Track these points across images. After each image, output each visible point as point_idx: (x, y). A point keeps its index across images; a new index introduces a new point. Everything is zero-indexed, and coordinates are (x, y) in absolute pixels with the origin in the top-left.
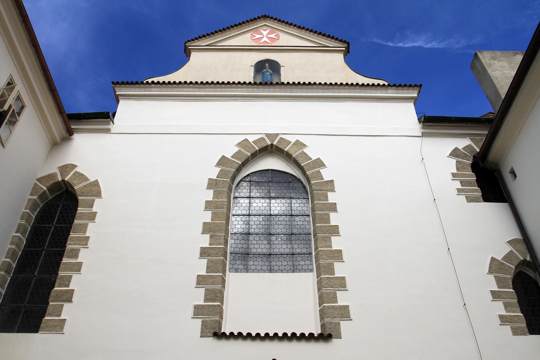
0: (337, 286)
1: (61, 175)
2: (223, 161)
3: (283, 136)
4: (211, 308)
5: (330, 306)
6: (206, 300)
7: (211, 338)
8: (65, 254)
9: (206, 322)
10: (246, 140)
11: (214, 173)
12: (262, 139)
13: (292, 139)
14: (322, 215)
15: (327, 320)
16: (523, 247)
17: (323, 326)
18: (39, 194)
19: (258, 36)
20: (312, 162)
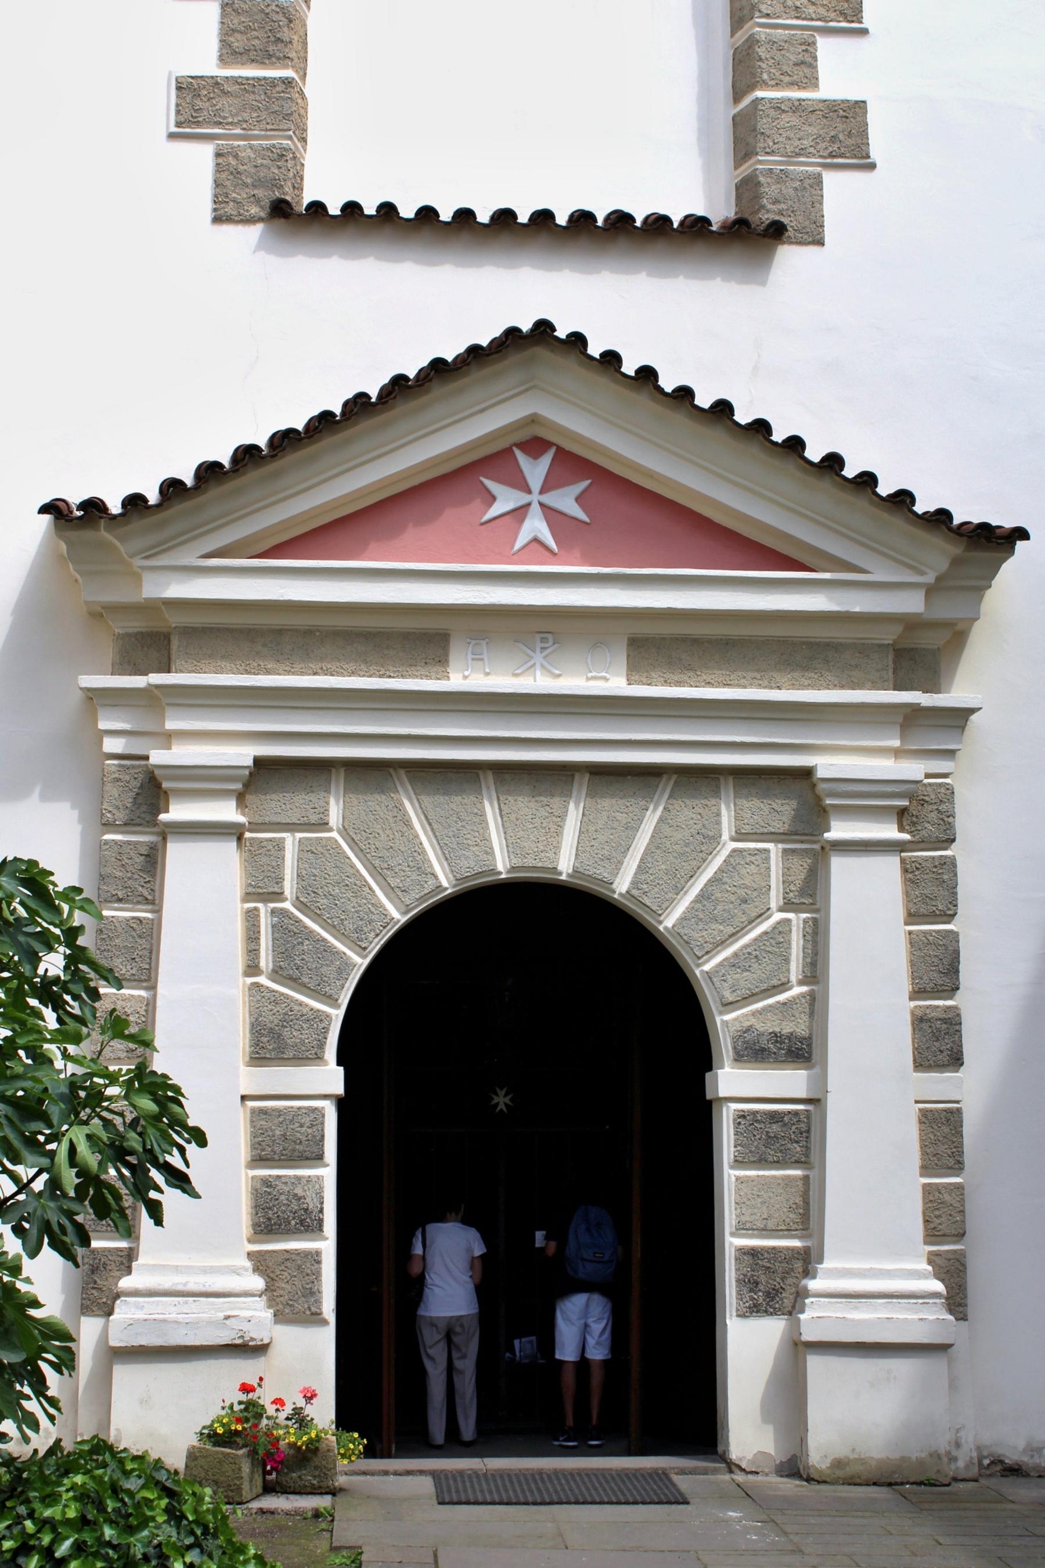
0: (822, 11)
4: (254, 93)
5: (782, 101)
6: (229, 53)
7: (259, 227)
9: (236, 156)
15: (764, 162)
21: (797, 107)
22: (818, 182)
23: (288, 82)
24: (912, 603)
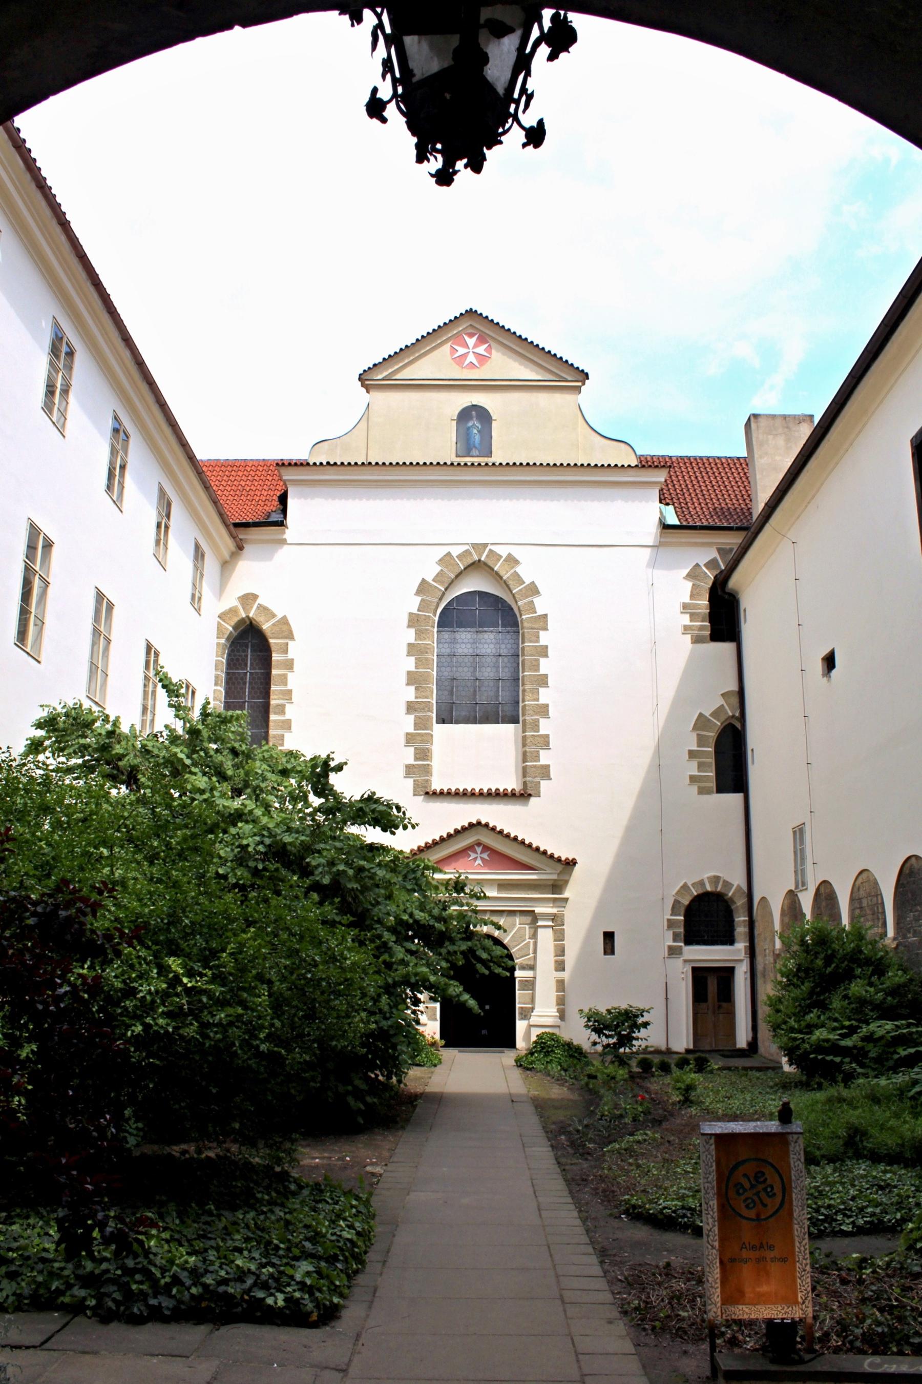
1: (244, 608)
2: (423, 588)
3: (493, 548)
6: (416, 759)
8: (271, 710)
10: (449, 554)
11: (413, 605)
12: (467, 551)
13: (503, 551)
14: (531, 661)
15: (528, 779)
16: (735, 700)
17: (525, 783)
18: (226, 636)
19: (461, 351)
20: (525, 587)
21: (535, 766)
22: (539, 783)
23: (428, 765)
24: (555, 877)
